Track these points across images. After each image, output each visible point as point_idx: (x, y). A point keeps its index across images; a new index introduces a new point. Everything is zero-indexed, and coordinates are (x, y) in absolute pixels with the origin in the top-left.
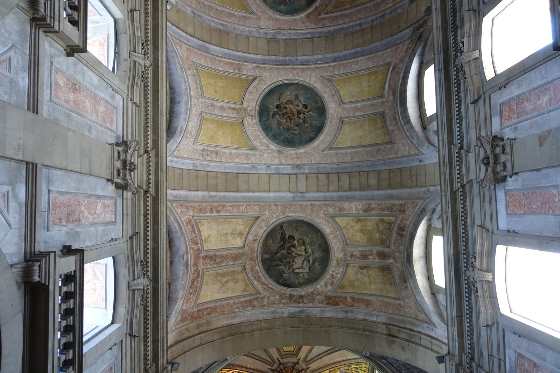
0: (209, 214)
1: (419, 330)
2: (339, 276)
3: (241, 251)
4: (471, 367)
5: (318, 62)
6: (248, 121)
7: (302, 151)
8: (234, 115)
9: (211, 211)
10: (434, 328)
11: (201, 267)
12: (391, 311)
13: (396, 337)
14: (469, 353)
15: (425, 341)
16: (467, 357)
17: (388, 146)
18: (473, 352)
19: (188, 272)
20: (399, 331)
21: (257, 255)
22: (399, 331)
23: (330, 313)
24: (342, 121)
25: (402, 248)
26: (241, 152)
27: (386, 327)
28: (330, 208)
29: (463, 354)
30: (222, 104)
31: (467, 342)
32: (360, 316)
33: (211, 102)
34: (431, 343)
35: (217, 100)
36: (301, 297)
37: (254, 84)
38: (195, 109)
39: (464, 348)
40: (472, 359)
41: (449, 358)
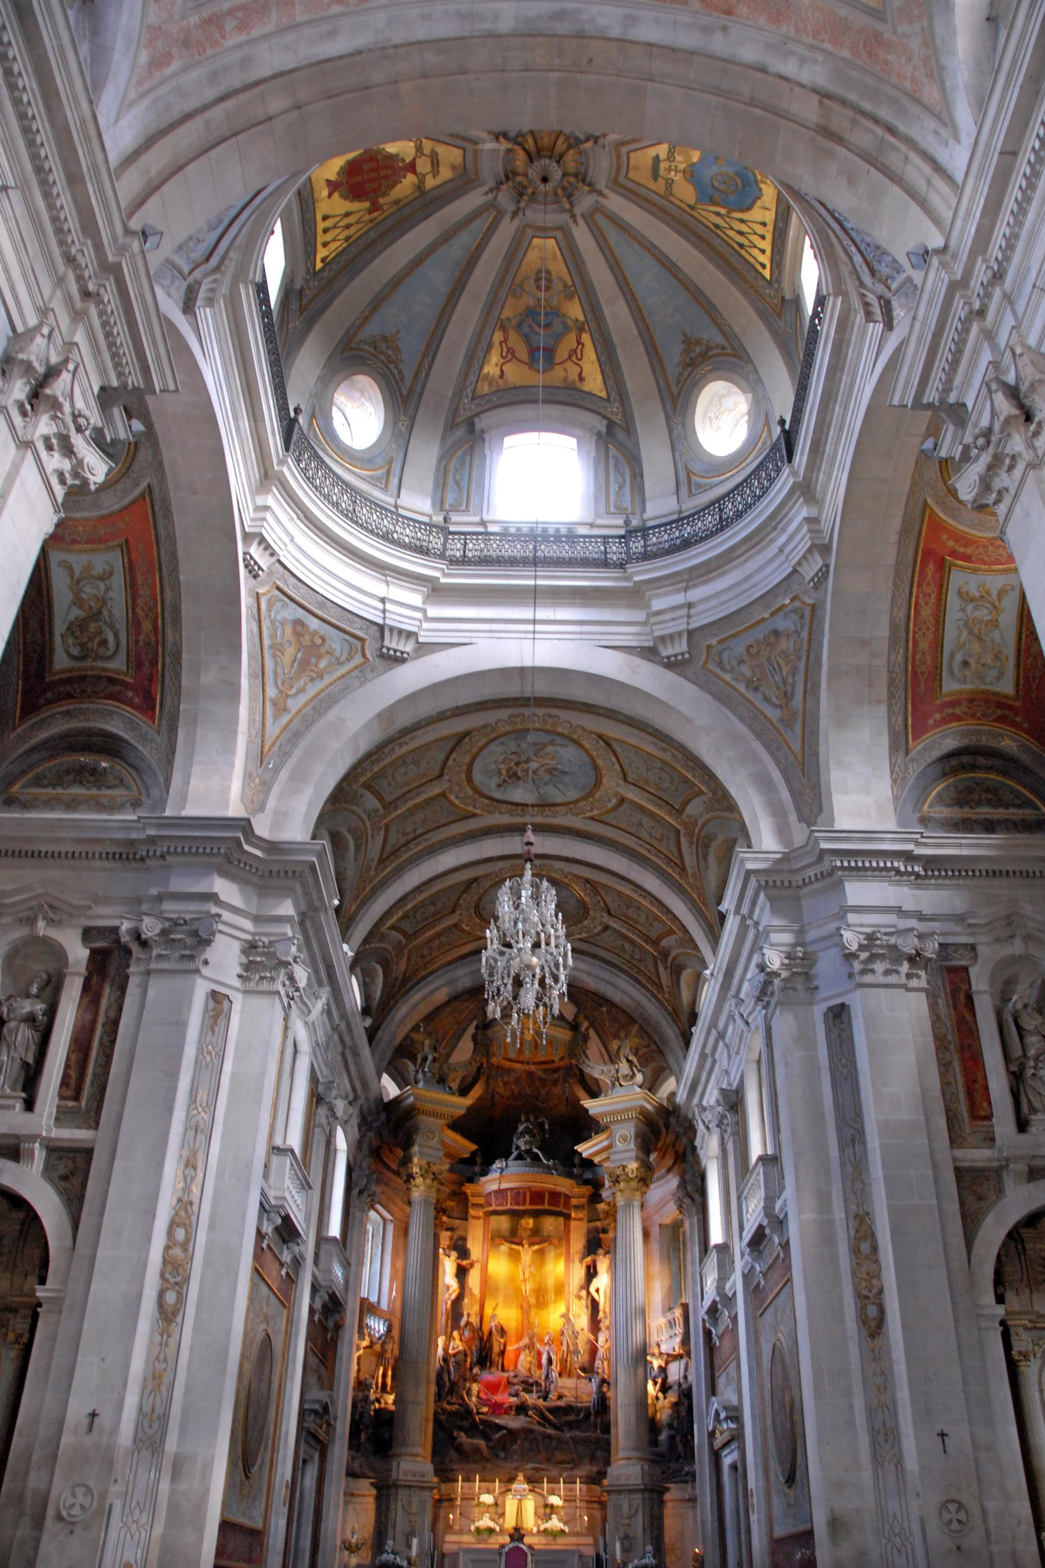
1: (913, 132)
4: (988, 295)
10: (951, 141)
12: (846, 53)
13: (840, 140)
14: (997, 259)
15: (916, 171)
16: (988, 268)
18: (1007, 259)
20: (854, 122)
22: (854, 122)
27: (821, 103)
29: (980, 259)
31: (1001, 230)
32: (749, 54)
34: (929, 182)
39: (988, 242)
40: (998, 276)
41: (940, 263)
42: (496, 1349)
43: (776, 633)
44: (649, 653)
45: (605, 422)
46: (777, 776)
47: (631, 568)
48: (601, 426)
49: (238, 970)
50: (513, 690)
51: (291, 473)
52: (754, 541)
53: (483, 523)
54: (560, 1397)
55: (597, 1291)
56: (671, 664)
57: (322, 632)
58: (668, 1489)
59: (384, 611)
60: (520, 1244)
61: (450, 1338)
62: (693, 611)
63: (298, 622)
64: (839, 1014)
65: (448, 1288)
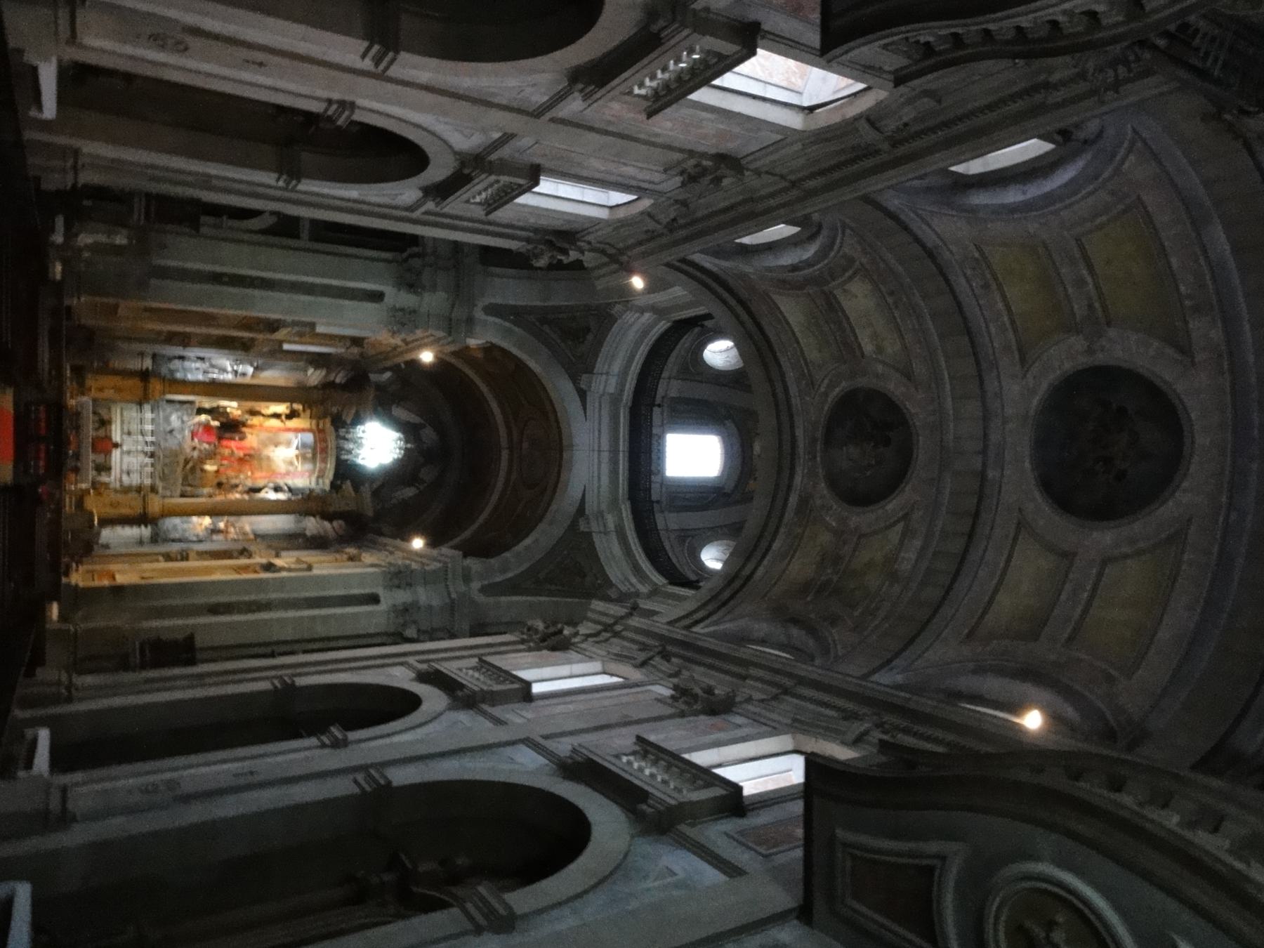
0: (883, 289)
2: (828, 519)
3: (858, 353)
5: (1233, 516)
6: (1077, 343)
7: (1027, 465)
8: (1079, 309)
9: (892, 293)
11: (811, 290)
17: (966, 631)
19: (789, 271)
21: (862, 382)
23: (793, 500)
24: (1068, 556)
25: (812, 616)
26: (1011, 335)
28: (921, 513)
30: (1089, 279)
33: (1078, 254)
35: (1090, 268)
36: (815, 457)
37: (1170, 351)
38: (1036, 225)
42: (234, 435)
43: (585, 576)
44: (581, 510)
45: (729, 492)
46: (510, 575)
47: (628, 504)
48: (728, 489)
49: (397, 306)
50: (565, 443)
51: (663, 326)
52: (637, 569)
53: (662, 425)
54: (203, 470)
55: (267, 492)
56: (573, 525)
57: (586, 342)
58: (146, 526)
59: (602, 374)
60: (297, 448)
61: (238, 409)
62: (603, 535)
63: (588, 330)
64: (374, 599)
65: (268, 407)
